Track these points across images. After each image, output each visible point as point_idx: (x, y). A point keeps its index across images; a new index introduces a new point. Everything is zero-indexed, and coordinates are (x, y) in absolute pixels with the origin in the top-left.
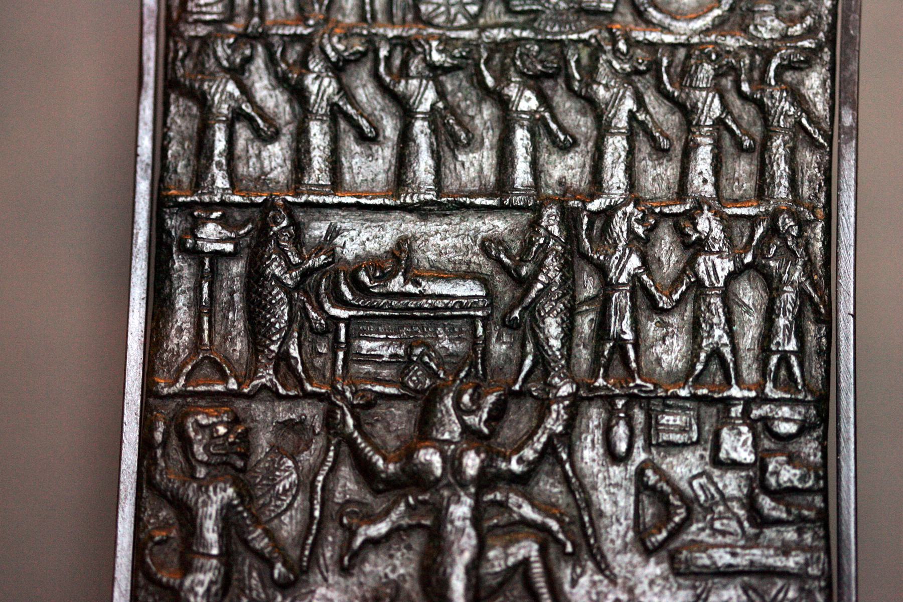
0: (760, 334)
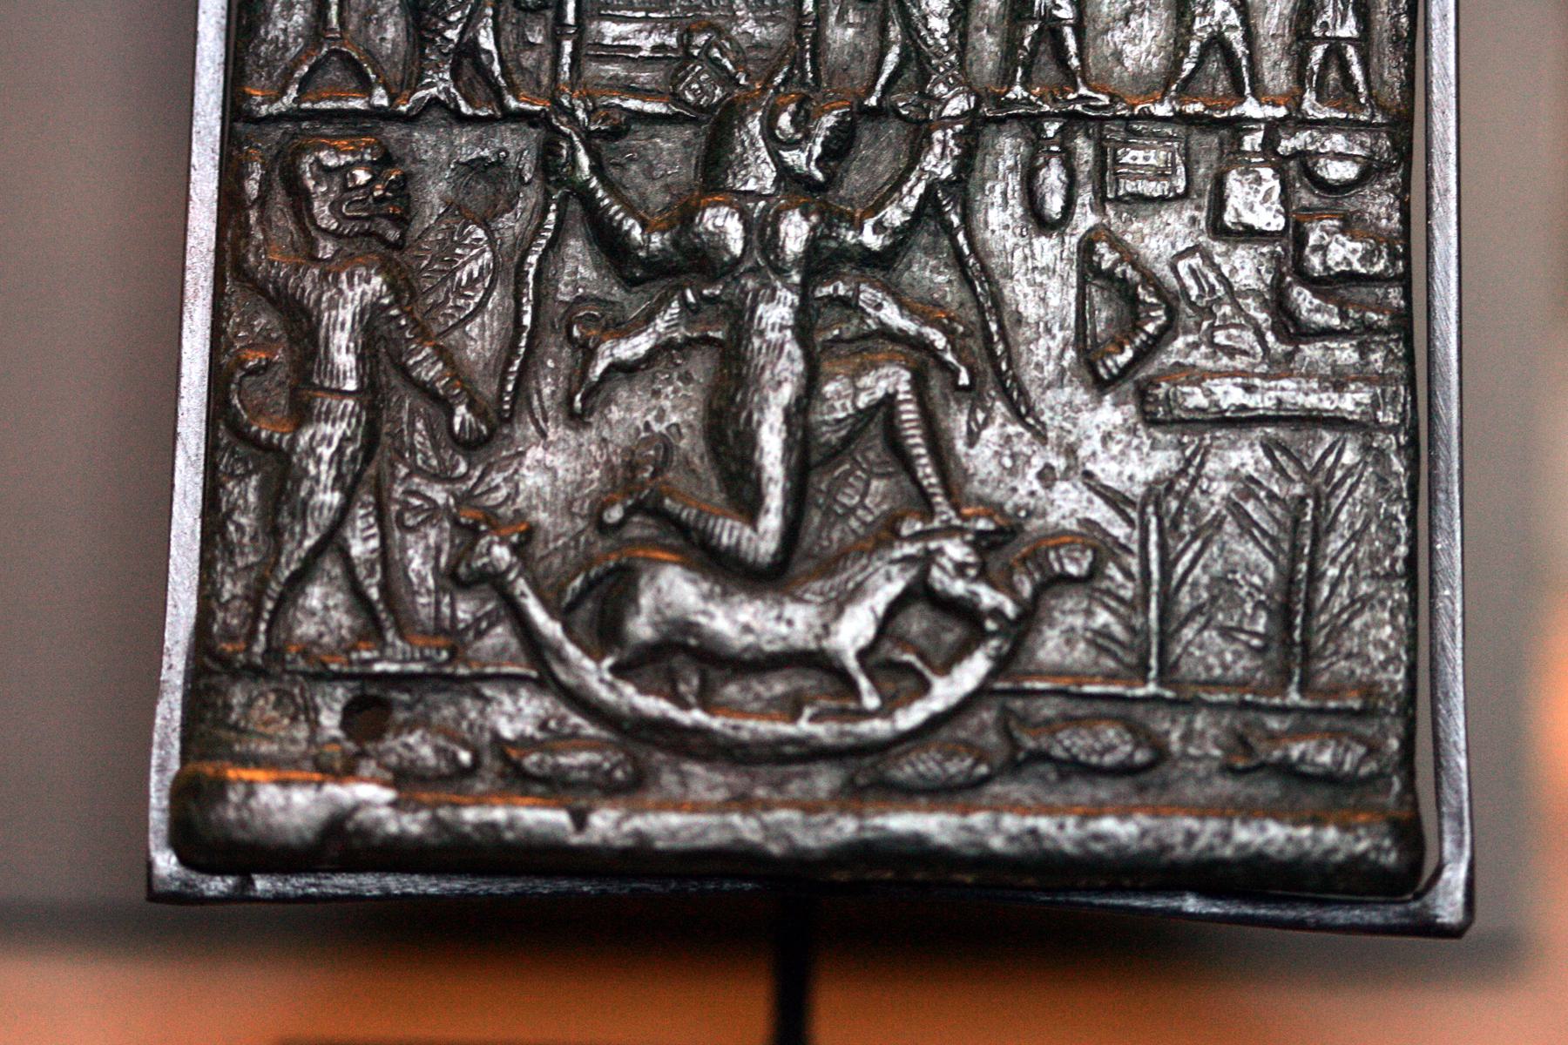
0: (1293, 9)
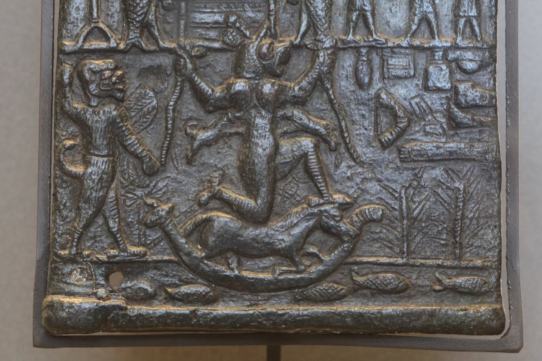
0: (453, 5)
